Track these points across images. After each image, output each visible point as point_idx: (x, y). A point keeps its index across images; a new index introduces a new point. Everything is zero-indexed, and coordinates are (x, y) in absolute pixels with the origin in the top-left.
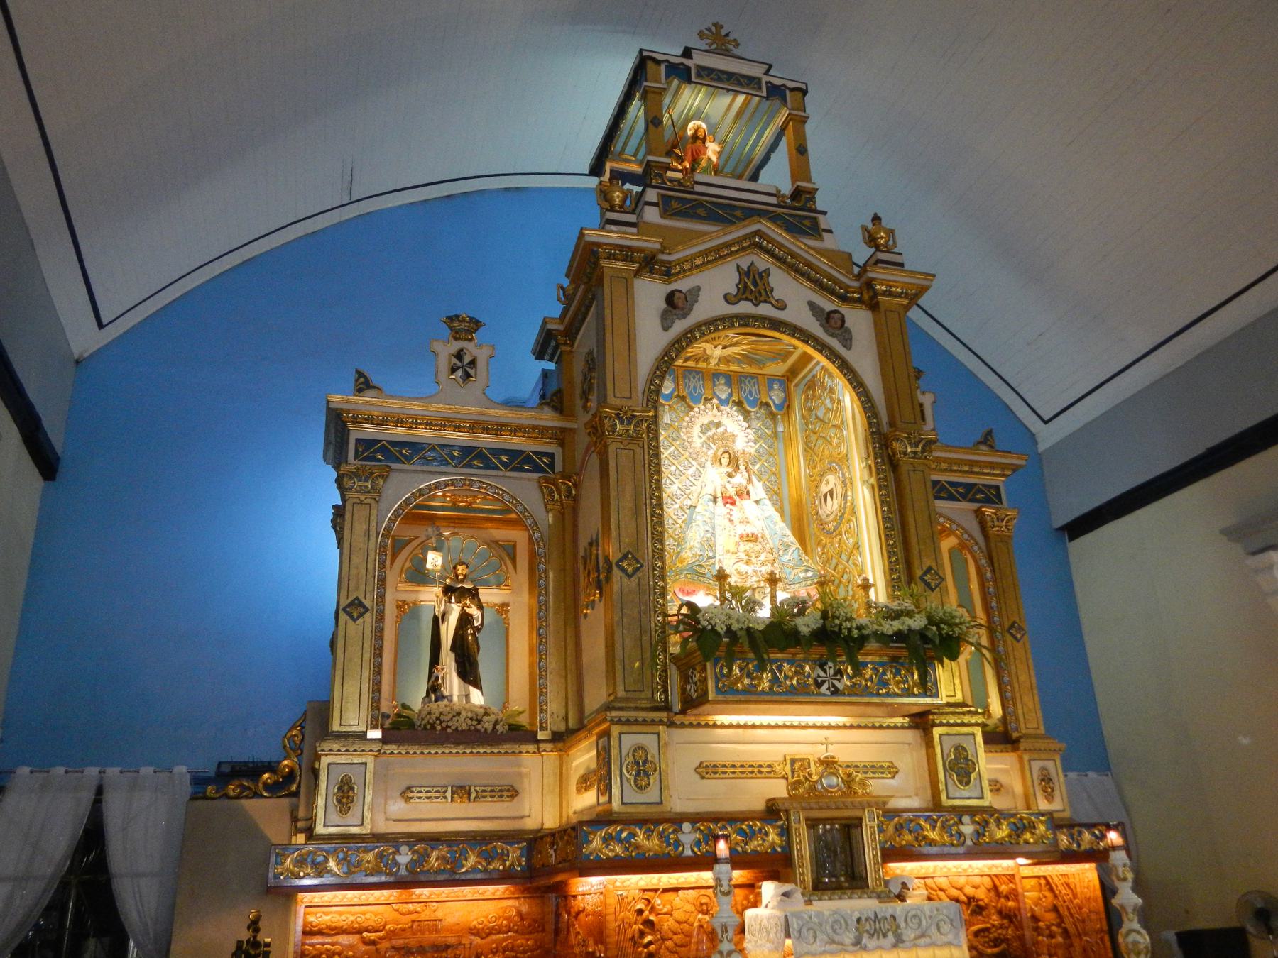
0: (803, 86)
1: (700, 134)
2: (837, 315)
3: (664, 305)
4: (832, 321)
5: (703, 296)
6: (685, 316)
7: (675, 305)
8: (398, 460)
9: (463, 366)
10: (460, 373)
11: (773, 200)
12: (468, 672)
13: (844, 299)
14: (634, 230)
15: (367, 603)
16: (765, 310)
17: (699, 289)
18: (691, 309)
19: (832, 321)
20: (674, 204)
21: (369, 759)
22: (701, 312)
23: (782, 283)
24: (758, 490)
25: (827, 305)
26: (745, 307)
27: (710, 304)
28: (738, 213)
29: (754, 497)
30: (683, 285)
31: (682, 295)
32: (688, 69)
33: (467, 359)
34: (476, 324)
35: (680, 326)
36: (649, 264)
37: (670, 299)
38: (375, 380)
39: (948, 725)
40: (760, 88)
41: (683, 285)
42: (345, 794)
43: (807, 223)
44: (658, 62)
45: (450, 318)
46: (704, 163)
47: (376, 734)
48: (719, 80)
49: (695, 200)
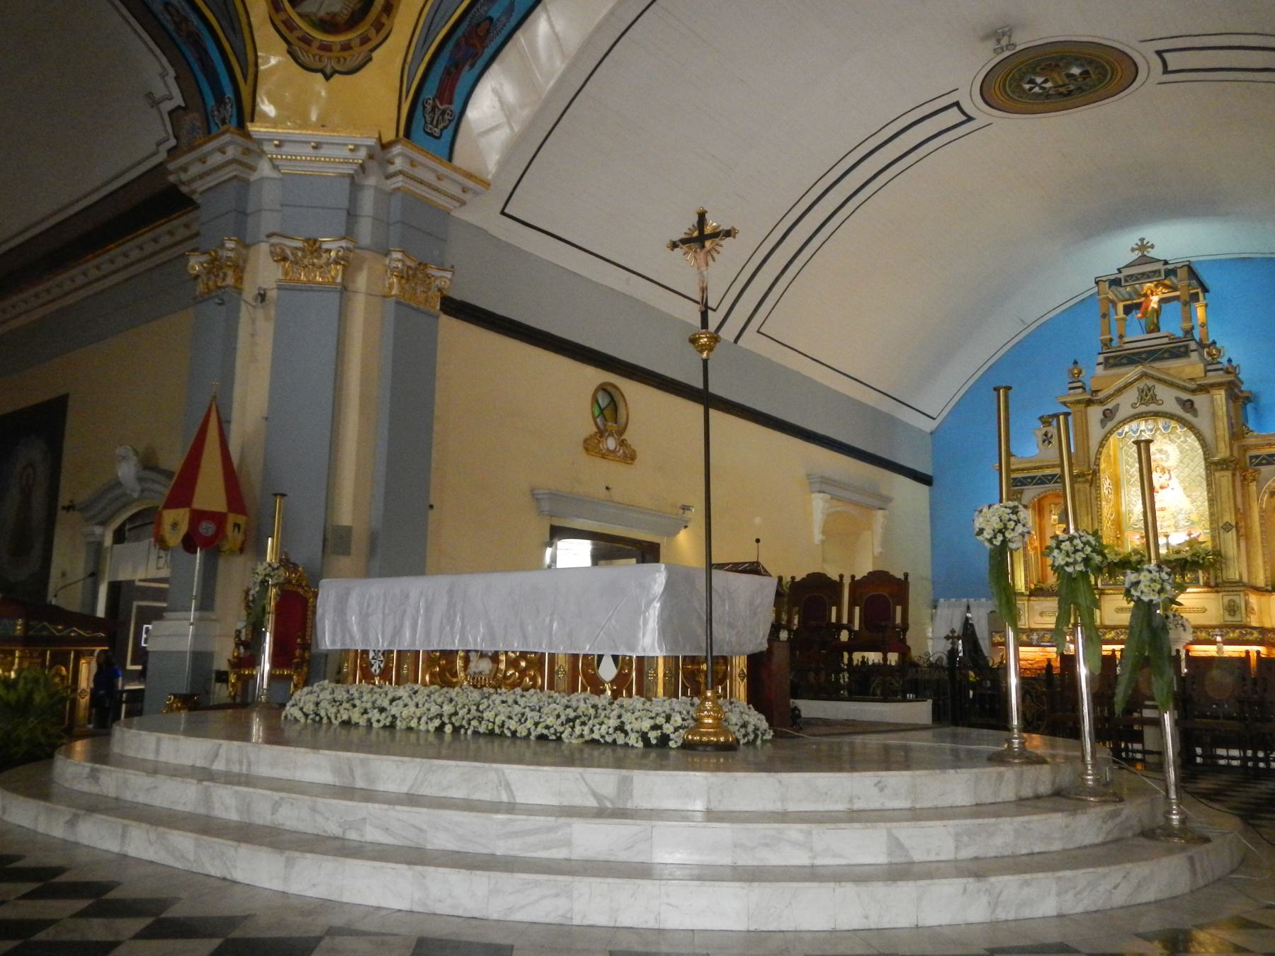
0: (1187, 263)
1: (1149, 292)
2: (1189, 403)
3: (1103, 417)
4: (1189, 406)
6: (1112, 420)
7: (1108, 415)
8: (1026, 485)
10: (1046, 442)
11: (1166, 340)
13: (1193, 391)
14: (1080, 390)
16: (1153, 407)
17: (1118, 405)
18: (1115, 415)
19: (1189, 406)
21: (1026, 603)
22: (1120, 416)
23: (1162, 392)
24: (1175, 483)
25: (1185, 396)
26: (1143, 408)
27: (1125, 411)
28: (1144, 356)
29: (1171, 487)
31: (1108, 412)
32: (1120, 279)
33: (1049, 435)
35: (1110, 425)
36: (1089, 402)
37: (1104, 413)
39: (1225, 591)
40: (1160, 276)
41: (1110, 406)
43: (1182, 349)
44: (1105, 281)
45: (1041, 418)
46: (1150, 308)
47: (1028, 593)
48: (1138, 279)
49: (1120, 356)
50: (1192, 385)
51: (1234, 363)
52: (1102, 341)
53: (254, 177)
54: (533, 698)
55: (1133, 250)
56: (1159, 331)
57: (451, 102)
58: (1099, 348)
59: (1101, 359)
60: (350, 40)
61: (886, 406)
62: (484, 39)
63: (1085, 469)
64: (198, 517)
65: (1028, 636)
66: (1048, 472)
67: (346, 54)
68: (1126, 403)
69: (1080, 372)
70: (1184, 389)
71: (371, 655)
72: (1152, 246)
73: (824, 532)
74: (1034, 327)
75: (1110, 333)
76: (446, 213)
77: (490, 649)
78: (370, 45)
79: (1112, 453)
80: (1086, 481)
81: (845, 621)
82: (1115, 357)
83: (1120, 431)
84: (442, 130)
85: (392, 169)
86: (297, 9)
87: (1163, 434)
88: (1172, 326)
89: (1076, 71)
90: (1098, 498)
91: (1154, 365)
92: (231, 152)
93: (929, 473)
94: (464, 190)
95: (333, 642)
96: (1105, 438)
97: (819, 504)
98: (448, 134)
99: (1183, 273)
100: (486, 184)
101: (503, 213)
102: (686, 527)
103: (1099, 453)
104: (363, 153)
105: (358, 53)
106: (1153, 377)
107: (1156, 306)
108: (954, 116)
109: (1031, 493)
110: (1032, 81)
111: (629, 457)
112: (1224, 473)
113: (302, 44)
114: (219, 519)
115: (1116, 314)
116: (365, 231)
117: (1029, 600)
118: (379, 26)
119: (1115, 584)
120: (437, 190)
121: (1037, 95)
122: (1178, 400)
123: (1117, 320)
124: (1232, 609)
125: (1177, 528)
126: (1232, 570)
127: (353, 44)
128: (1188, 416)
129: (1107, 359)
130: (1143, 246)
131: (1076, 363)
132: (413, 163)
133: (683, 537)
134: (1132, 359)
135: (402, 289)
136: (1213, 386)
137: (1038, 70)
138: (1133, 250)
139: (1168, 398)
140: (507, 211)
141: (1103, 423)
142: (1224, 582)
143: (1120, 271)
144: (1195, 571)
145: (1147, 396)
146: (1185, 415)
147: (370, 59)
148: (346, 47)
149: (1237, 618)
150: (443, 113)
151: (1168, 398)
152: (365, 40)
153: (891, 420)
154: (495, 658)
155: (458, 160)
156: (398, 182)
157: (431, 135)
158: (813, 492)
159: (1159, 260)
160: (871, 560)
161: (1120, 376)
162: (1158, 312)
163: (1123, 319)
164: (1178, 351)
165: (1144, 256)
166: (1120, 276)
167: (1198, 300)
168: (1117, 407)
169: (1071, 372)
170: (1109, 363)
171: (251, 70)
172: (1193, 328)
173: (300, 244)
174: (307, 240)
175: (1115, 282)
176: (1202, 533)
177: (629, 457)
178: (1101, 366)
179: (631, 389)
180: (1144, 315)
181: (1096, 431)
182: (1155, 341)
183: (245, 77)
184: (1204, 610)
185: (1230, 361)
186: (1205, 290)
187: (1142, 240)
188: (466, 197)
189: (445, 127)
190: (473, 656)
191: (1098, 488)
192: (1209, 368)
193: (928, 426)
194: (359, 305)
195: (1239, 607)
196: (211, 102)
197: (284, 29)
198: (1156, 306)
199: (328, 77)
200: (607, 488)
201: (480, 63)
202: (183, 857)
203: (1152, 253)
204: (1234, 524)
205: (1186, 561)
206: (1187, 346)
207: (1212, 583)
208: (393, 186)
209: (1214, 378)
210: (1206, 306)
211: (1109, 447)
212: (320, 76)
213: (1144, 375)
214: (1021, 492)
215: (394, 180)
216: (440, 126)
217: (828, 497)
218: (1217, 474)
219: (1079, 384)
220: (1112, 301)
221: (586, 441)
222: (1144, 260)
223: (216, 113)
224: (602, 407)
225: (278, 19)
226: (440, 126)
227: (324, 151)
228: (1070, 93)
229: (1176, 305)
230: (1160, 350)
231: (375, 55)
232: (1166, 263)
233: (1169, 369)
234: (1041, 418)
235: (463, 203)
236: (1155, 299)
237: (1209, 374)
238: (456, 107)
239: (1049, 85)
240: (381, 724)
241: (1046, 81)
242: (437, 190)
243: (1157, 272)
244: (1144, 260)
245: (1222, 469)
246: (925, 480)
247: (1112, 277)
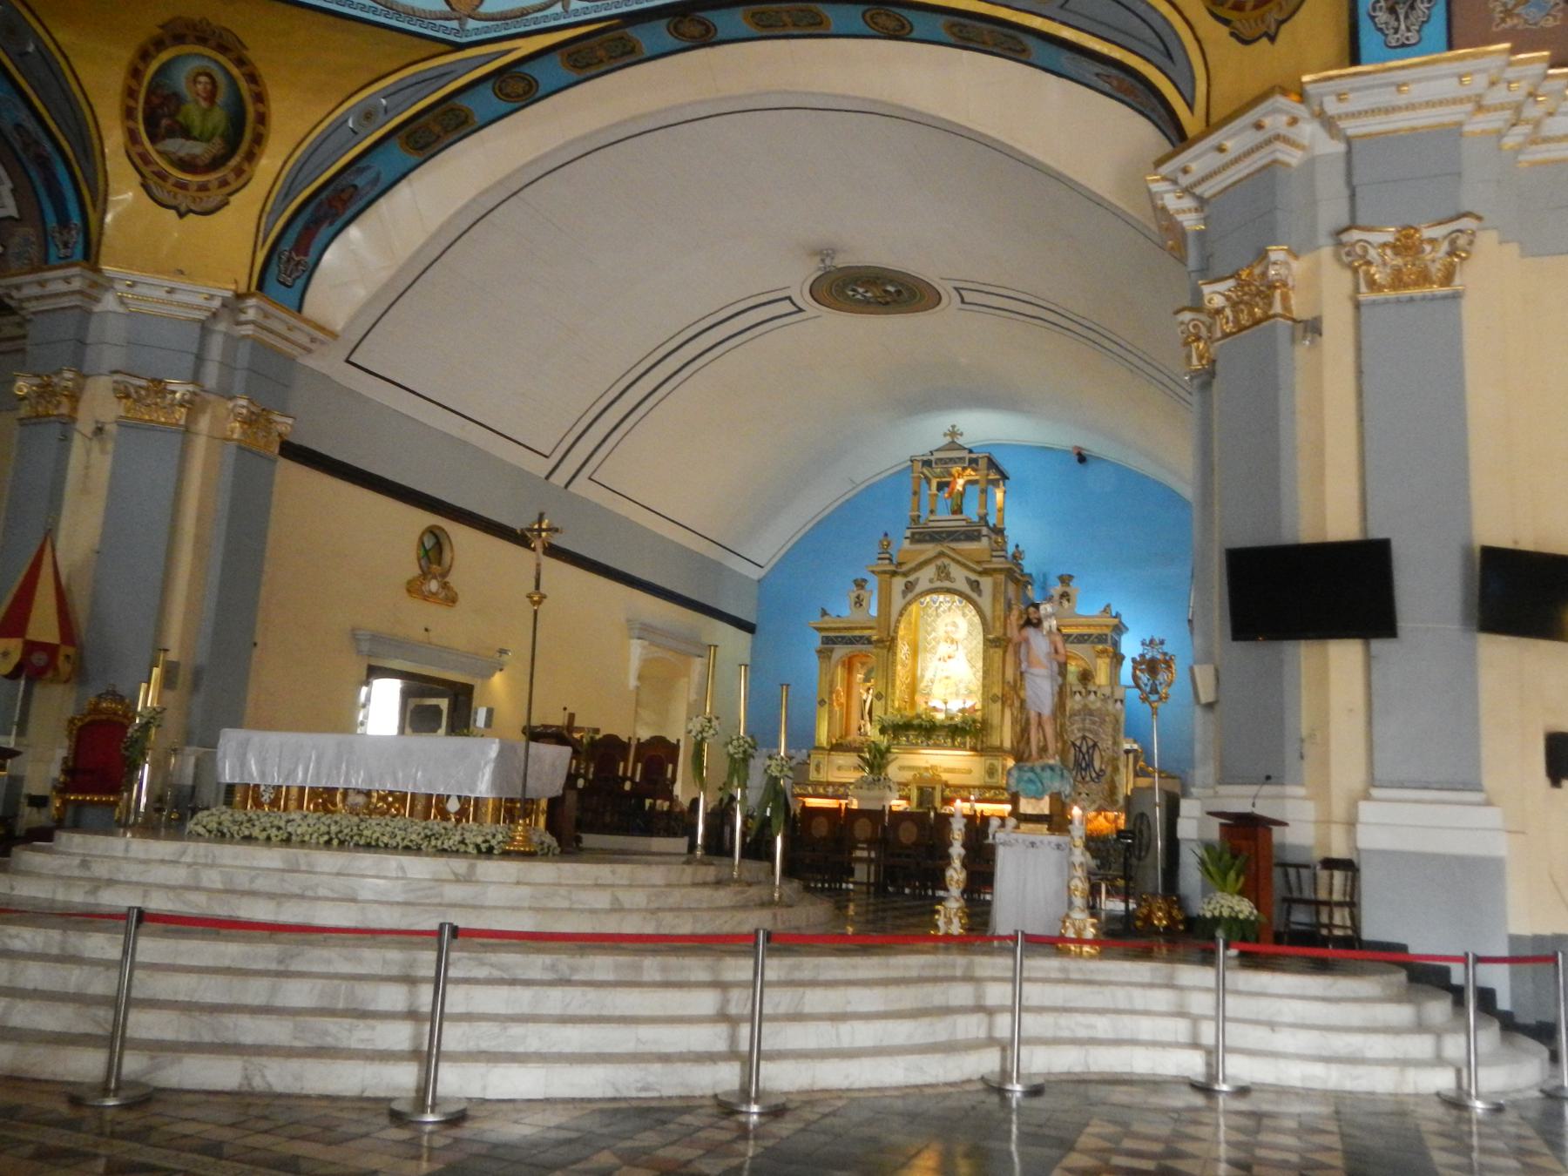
3: (903, 588)
4: (975, 586)
5: (920, 582)
6: (911, 591)
7: (909, 587)
9: (859, 602)
11: (964, 523)
13: (980, 573)
14: (887, 561)
15: (826, 700)
16: (947, 584)
19: (975, 586)
20: (917, 537)
22: (918, 589)
25: (974, 577)
26: (938, 584)
28: (944, 535)
30: (911, 578)
34: (865, 581)
35: (910, 596)
36: (894, 574)
38: (828, 612)
41: (911, 578)
42: (818, 768)
43: (976, 534)
47: (828, 747)
50: (979, 568)
51: (1021, 549)
52: (911, 516)
53: (98, 308)
54: (399, 822)
55: (945, 435)
56: (961, 513)
57: (306, 254)
58: (907, 522)
59: (908, 533)
60: (208, 181)
61: (714, 553)
62: (345, 204)
63: (884, 635)
64: (31, 647)
65: (824, 789)
66: (857, 633)
67: (201, 194)
68: (926, 576)
69: (888, 545)
70: (974, 571)
71: (262, 788)
72: (961, 434)
73: (640, 678)
74: (863, 486)
75: (918, 510)
76: (292, 359)
77: (365, 787)
78: (228, 189)
79: (913, 621)
80: (885, 647)
81: (629, 774)
82: (921, 533)
83: (922, 600)
84: (294, 280)
85: (243, 317)
86: (160, 146)
87: (958, 607)
88: (972, 511)
89: (891, 289)
90: (894, 663)
91: (953, 545)
92: (77, 284)
93: (751, 618)
94: (313, 340)
95: (232, 777)
96: (904, 608)
97: (636, 650)
98: (300, 283)
99: (983, 464)
100: (334, 335)
101: (348, 361)
102: (501, 670)
103: (898, 621)
104: (216, 303)
105: (216, 196)
106: (949, 557)
107: (961, 489)
108: (786, 307)
109: (841, 651)
110: (854, 290)
111: (451, 600)
112: (997, 650)
113: (155, 178)
114: (50, 649)
115: (930, 489)
116: (211, 375)
117: (829, 754)
118: (239, 172)
119: (898, 744)
120: (287, 339)
121: (859, 300)
122: (968, 580)
123: (930, 495)
124: (991, 772)
125: (957, 695)
126: (994, 737)
127: (210, 186)
128: (974, 596)
129: (913, 534)
130: (953, 433)
131: (886, 535)
132: (266, 315)
133: (498, 680)
134: (934, 536)
135: (244, 433)
136: (995, 570)
137: (859, 283)
138: (945, 435)
139: (960, 576)
140: (352, 359)
141: (904, 593)
142: (988, 747)
143: (932, 453)
144: (964, 737)
145: (943, 573)
146: (973, 592)
147: (227, 203)
148: (203, 188)
149: (994, 780)
150: (298, 263)
151: (960, 576)
152: (224, 183)
153: (718, 567)
154: (368, 794)
155: (309, 309)
156: (248, 330)
157: (283, 284)
158: (631, 638)
159: (965, 449)
160: (685, 707)
161: (922, 552)
162: (962, 494)
163: (936, 495)
164: (972, 535)
165: (953, 442)
166: (932, 458)
167: (998, 487)
168: (918, 579)
169: (881, 542)
170: (916, 538)
171: (101, 198)
172: (986, 514)
173: (143, 383)
174: (153, 380)
175: (927, 463)
176: (974, 701)
177: (451, 600)
178: (908, 541)
179: (460, 534)
180: (951, 495)
181: (897, 601)
182: (956, 523)
183: (94, 206)
184: (970, 772)
185: (1017, 546)
186: (1004, 477)
187: (953, 427)
188: (313, 346)
189: (298, 277)
190: (350, 792)
191: (895, 654)
192: (994, 553)
193: (755, 574)
194: (200, 445)
195: (997, 770)
196: (52, 221)
197: (140, 162)
198: (961, 489)
199: (181, 215)
200: (426, 630)
201: (338, 224)
202: (197, 906)
203: (960, 441)
204: (1000, 695)
205: (956, 726)
206: (979, 531)
207: (979, 747)
208: (243, 333)
209: (998, 563)
210: (1005, 492)
211: (910, 615)
212: (172, 213)
213: (941, 554)
214: (832, 651)
215: (244, 327)
216: (293, 276)
217: (646, 643)
218: (992, 651)
219: (887, 556)
220: (926, 477)
221: (409, 582)
222: (952, 446)
223: (57, 235)
224: (427, 548)
225: (134, 151)
226: (293, 276)
227: (177, 297)
228: (887, 303)
229: (977, 488)
230: (957, 531)
231: (233, 199)
232: (971, 451)
233: (963, 550)
235: (309, 351)
236: (961, 482)
237: (994, 559)
238: (310, 259)
239: (869, 295)
240: (279, 838)
241: (866, 292)
242: (287, 339)
243: (961, 459)
244: (952, 446)
245: (996, 647)
246: (749, 628)
247: (925, 458)
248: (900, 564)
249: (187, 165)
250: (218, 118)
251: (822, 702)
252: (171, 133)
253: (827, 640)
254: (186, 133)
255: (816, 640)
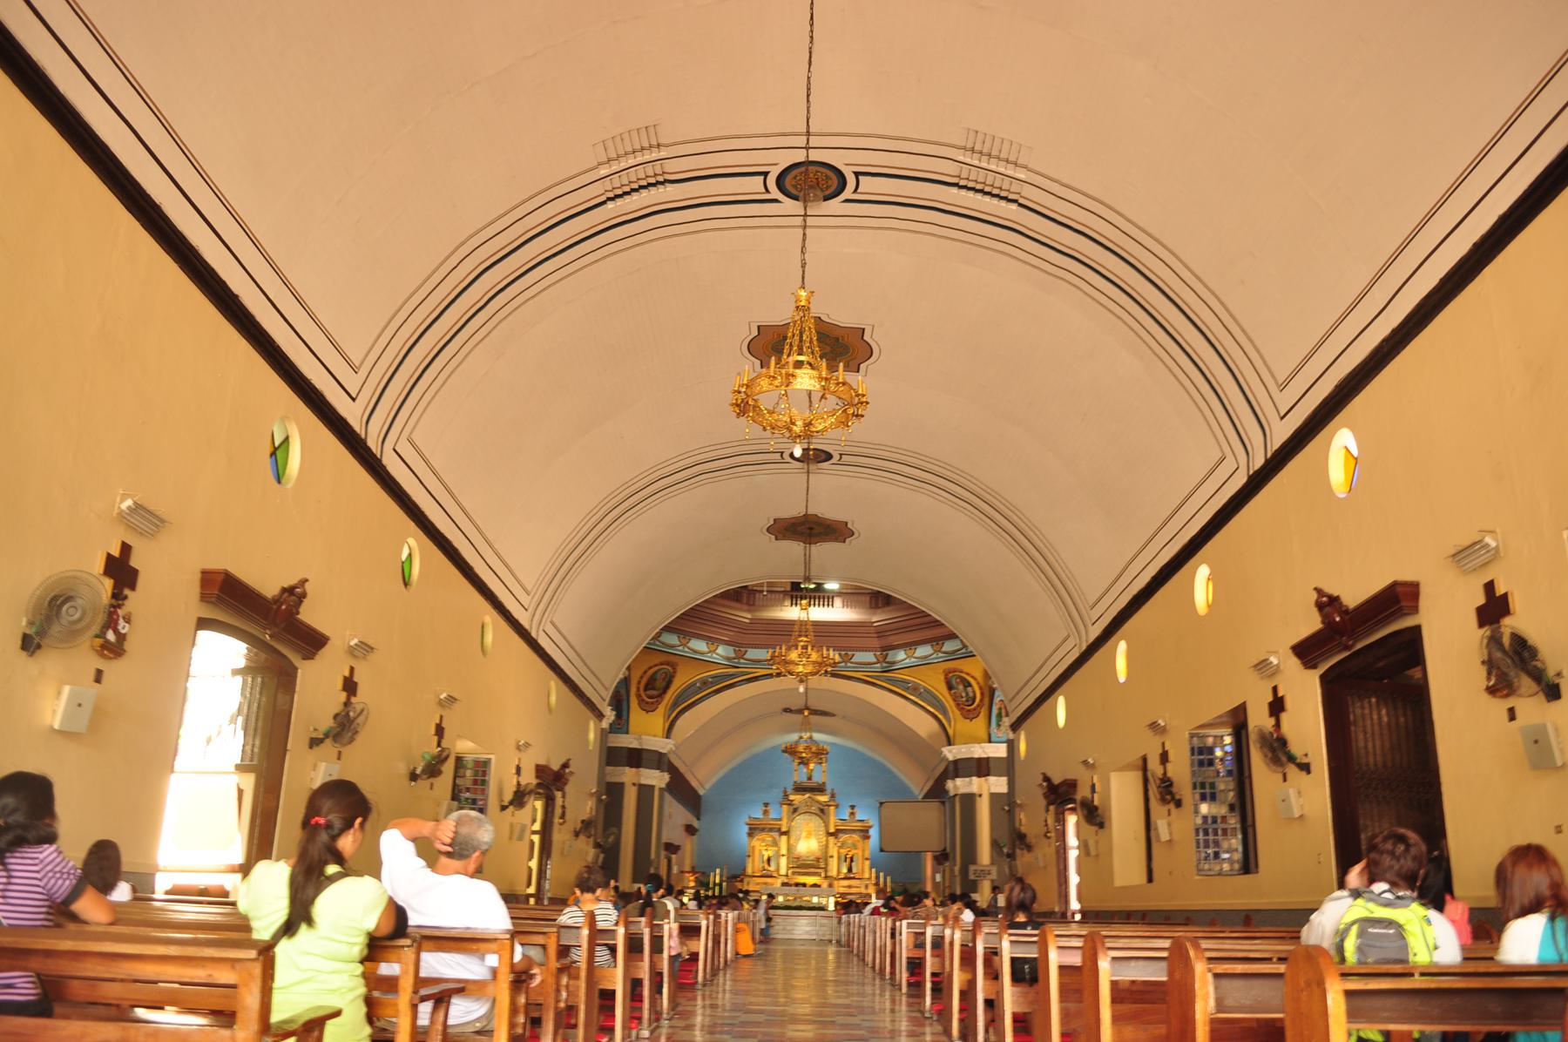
4: (822, 811)
12: (769, 864)
19: (822, 811)
22: (800, 811)
45: (765, 804)
78: (659, 703)
105: (654, 706)
148: (652, 703)
197: (639, 696)
234: (765, 804)
248: (792, 801)
249: (650, 697)
250: (664, 684)
251: (749, 856)
252: (650, 689)
253: (750, 829)
254: (654, 689)
255: (746, 829)
